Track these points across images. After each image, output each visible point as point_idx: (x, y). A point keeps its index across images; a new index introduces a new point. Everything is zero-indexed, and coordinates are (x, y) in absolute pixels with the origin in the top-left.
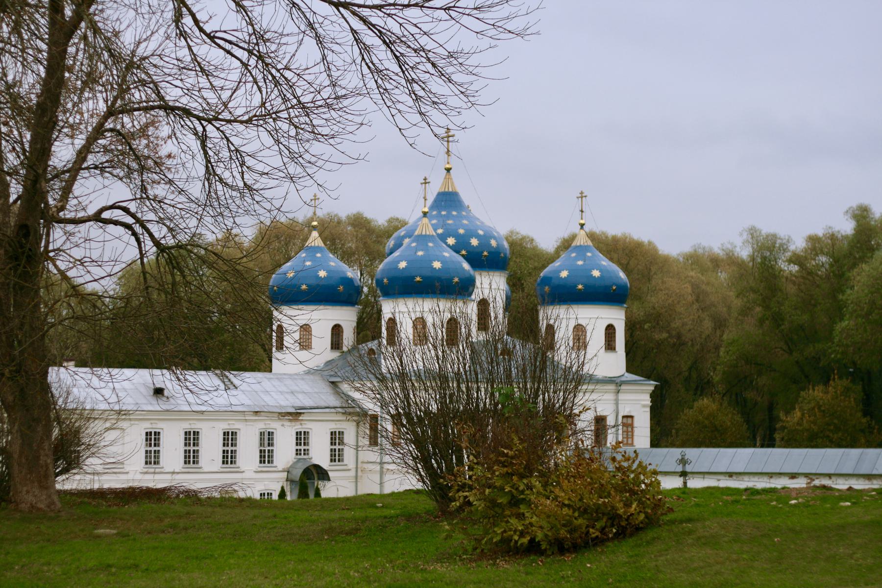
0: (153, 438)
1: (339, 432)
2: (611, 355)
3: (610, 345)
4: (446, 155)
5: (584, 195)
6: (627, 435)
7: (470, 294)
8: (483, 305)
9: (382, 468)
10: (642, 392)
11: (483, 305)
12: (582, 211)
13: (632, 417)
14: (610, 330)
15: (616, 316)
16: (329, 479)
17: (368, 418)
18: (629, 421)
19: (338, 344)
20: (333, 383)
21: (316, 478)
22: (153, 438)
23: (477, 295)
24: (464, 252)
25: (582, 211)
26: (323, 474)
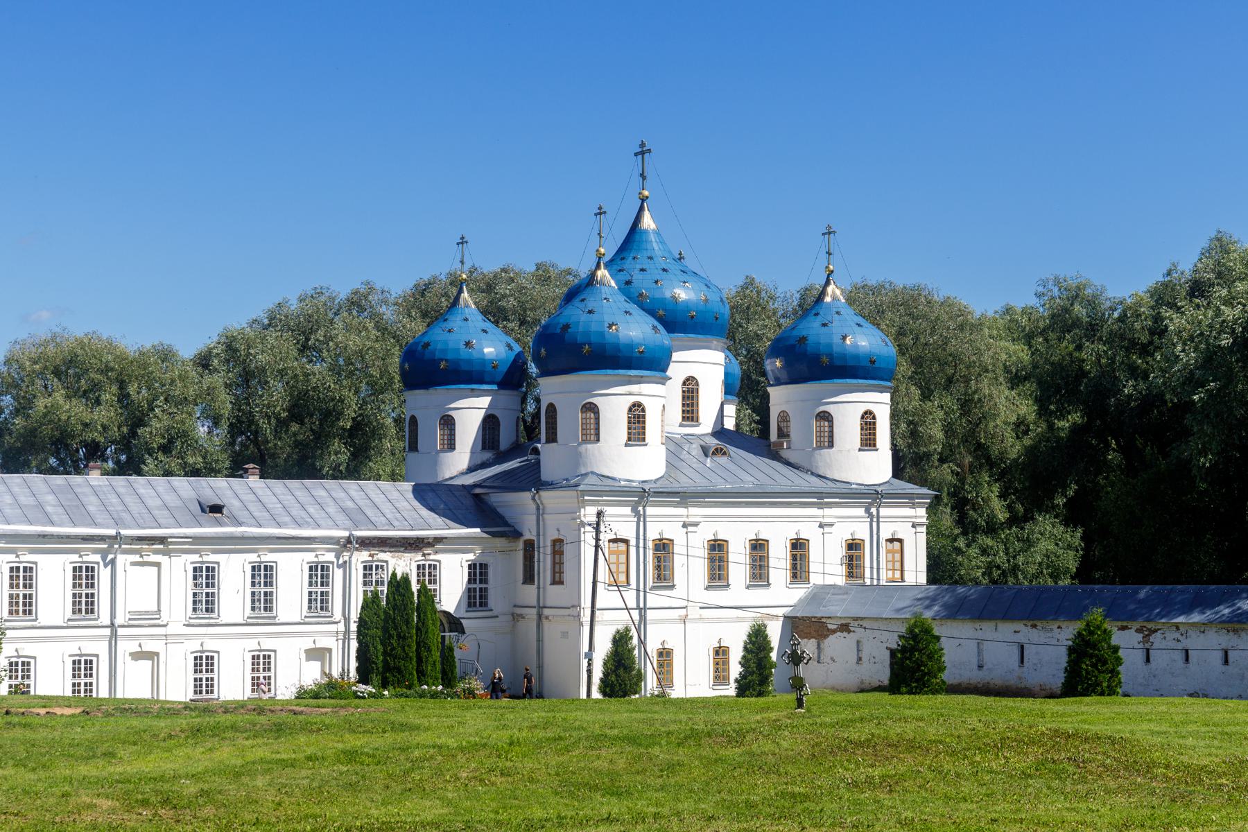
0: (206, 576)
1: (481, 565)
2: (868, 455)
3: (869, 441)
4: (641, 179)
5: (831, 230)
6: (894, 566)
7: (664, 370)
8: (690, 390)
9: (540, 616)
10: (913, 506)
11: (690, 390)
12: (829, 253)
13: (900, 541)
14: (868, 421)
15: (880, 403)
16: (463, 632)
17: (521, 545)
18: (897, 545)
19: (493, 443)
20: (477, 496)
21: (447, 629)
22: (206, 576)
23: (678, 371)
24: (661, 312)
25: (829, 253)
26: (455, 623)
